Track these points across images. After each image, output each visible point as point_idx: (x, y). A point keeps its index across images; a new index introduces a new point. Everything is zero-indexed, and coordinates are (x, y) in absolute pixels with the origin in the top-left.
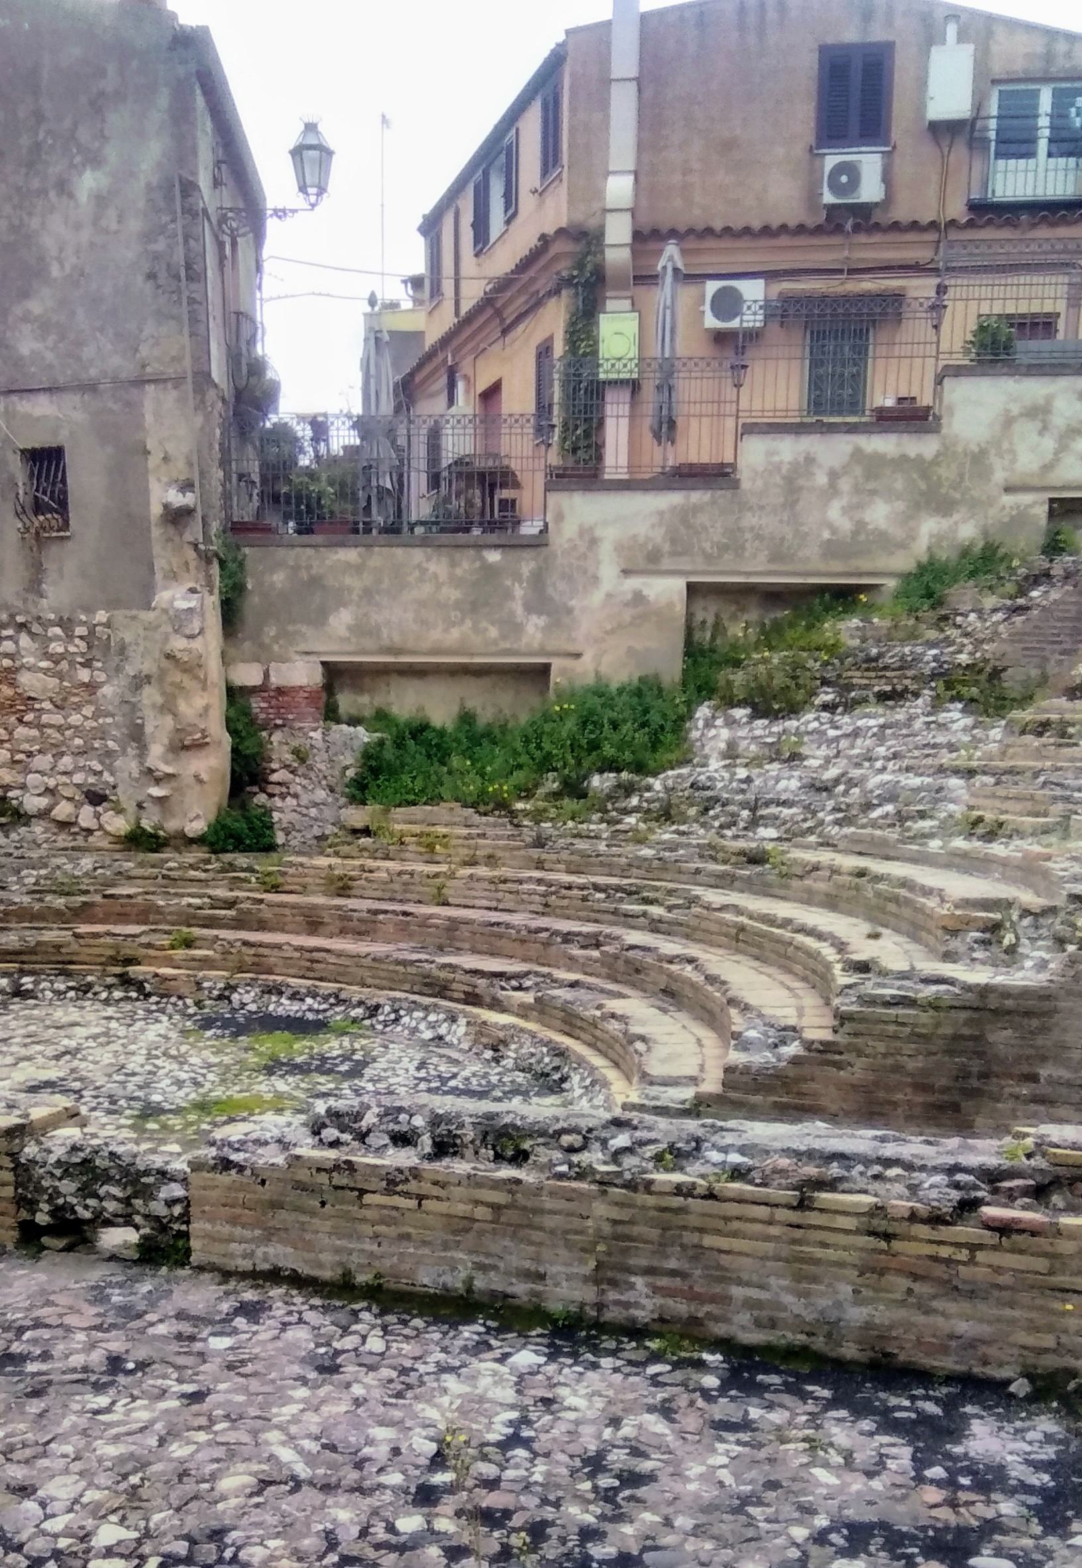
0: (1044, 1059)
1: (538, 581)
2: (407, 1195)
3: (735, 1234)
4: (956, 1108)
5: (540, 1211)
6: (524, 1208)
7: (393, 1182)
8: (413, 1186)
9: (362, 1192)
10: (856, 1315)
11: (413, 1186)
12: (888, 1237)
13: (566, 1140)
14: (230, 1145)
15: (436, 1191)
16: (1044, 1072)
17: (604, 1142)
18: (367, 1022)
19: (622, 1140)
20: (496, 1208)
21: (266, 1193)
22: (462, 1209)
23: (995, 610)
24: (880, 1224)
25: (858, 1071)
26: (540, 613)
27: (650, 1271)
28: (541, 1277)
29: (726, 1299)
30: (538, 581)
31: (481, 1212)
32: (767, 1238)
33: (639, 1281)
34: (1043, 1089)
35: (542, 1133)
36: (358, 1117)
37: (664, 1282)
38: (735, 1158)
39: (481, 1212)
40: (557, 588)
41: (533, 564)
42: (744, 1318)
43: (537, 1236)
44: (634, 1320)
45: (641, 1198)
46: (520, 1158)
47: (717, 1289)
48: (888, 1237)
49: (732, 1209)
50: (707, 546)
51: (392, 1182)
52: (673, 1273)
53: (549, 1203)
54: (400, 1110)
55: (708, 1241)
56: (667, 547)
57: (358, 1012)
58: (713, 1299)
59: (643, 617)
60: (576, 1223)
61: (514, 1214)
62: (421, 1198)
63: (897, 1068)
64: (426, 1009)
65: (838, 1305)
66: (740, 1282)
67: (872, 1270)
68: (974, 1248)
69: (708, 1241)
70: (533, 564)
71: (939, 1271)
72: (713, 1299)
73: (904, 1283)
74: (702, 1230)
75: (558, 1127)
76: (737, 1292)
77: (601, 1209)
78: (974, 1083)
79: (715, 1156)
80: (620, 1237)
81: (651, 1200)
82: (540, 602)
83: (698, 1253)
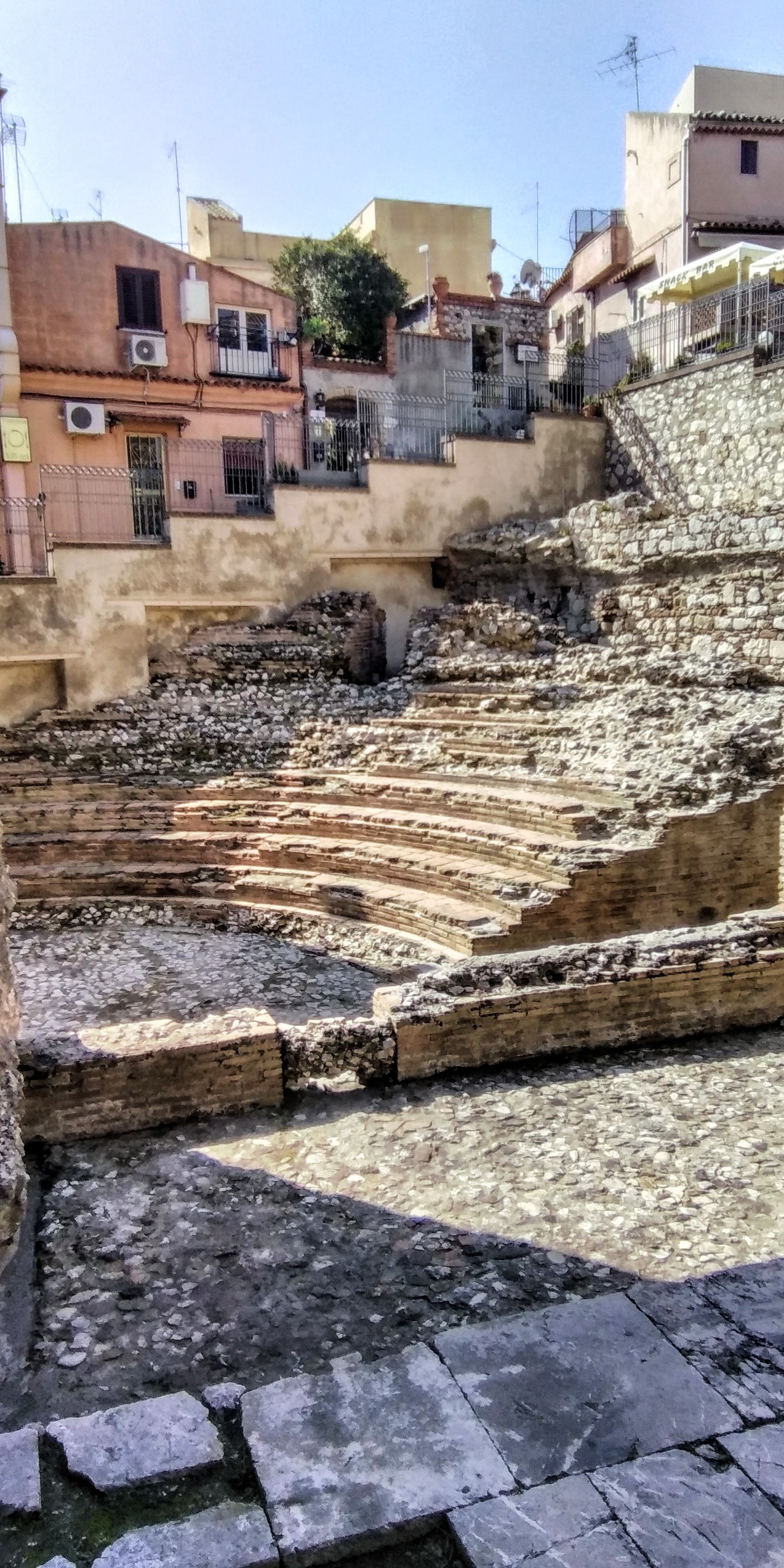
0: (657, 879)
1: (51, 607)
2: (521, 1011)
3: (672, 990)
4: (624, 908)
5: (586, 1002)
6: (579, 1003)
7: (512, 1005)
8: (523, 1006)
9: (496, 1015)
10: (721, 1012)
11: (523, 1006)
12: (731, 975)
13: (580, 963)
14: (408, 1009)
15: (535, 1005)
16: (658, 885)
17: (595, 961)
18: (76, 921)
19: (602, 958)
20: (564, 1005)
21: (445, 1027)
22: (549, 1011)
23: (335, 624)
24: (728, 971)
25: (582, 899)
26: (54, 627)
27: (638, 1015)
28: (587, 1033)
29: (669, 1020)
30: (51, 607)
31: (558, 1010)
32: (685, 988)
33: (632, 1023)
34: (659, 892)
35: (566, 963)
36: (470, 977)
37: (643, 1019)
38: (656, 956)
39: (558, 1010)
40: (63, 611)
41: (47, 597)
42: (676, 1027)
43: (585, 1014)
44: (630, 1042)
45: (633, 983)
46: (559, 978)
47: (666, 1015)
48: (731, 975)
49: (670, 978)
50: (155, 584)
51: (512, 1006)
52: (647, 1014)
53: (590, 997)
54: (485, 967)
55: (661, 995)
56: (132, 585)
57: (64, 915)
58: (663, 1022)
59: (122, 628)
60: (604, 1003)
61: (575, 1004)
62: (527, 1010)
63: (599, 895)
64: (130, 905)
65: (714, 1009)
66: (674, 1009)
67: (726, 990)
68: (761, 970)
69: (661, 995)
70: (47, 597)
71: (750, 984)
72: (663, 1022)
73: (738, 993)
74: (658, 992)
75: (570, 958)
76: (673, 1015)
77: (616, 993)
78: (631, 896)
79: (647, 956)
80: (624, 1005)
81: (636, 983)
82: (54, 620)
83: (656, 1003)
